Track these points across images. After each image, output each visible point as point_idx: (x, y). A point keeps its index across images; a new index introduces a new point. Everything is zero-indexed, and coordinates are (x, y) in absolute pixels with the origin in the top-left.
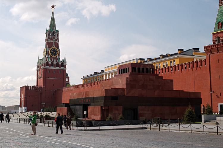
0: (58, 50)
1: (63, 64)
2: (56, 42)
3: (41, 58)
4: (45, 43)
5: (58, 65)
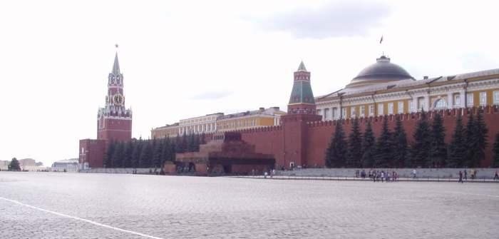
1: (128, 114)
5: (123, 115)
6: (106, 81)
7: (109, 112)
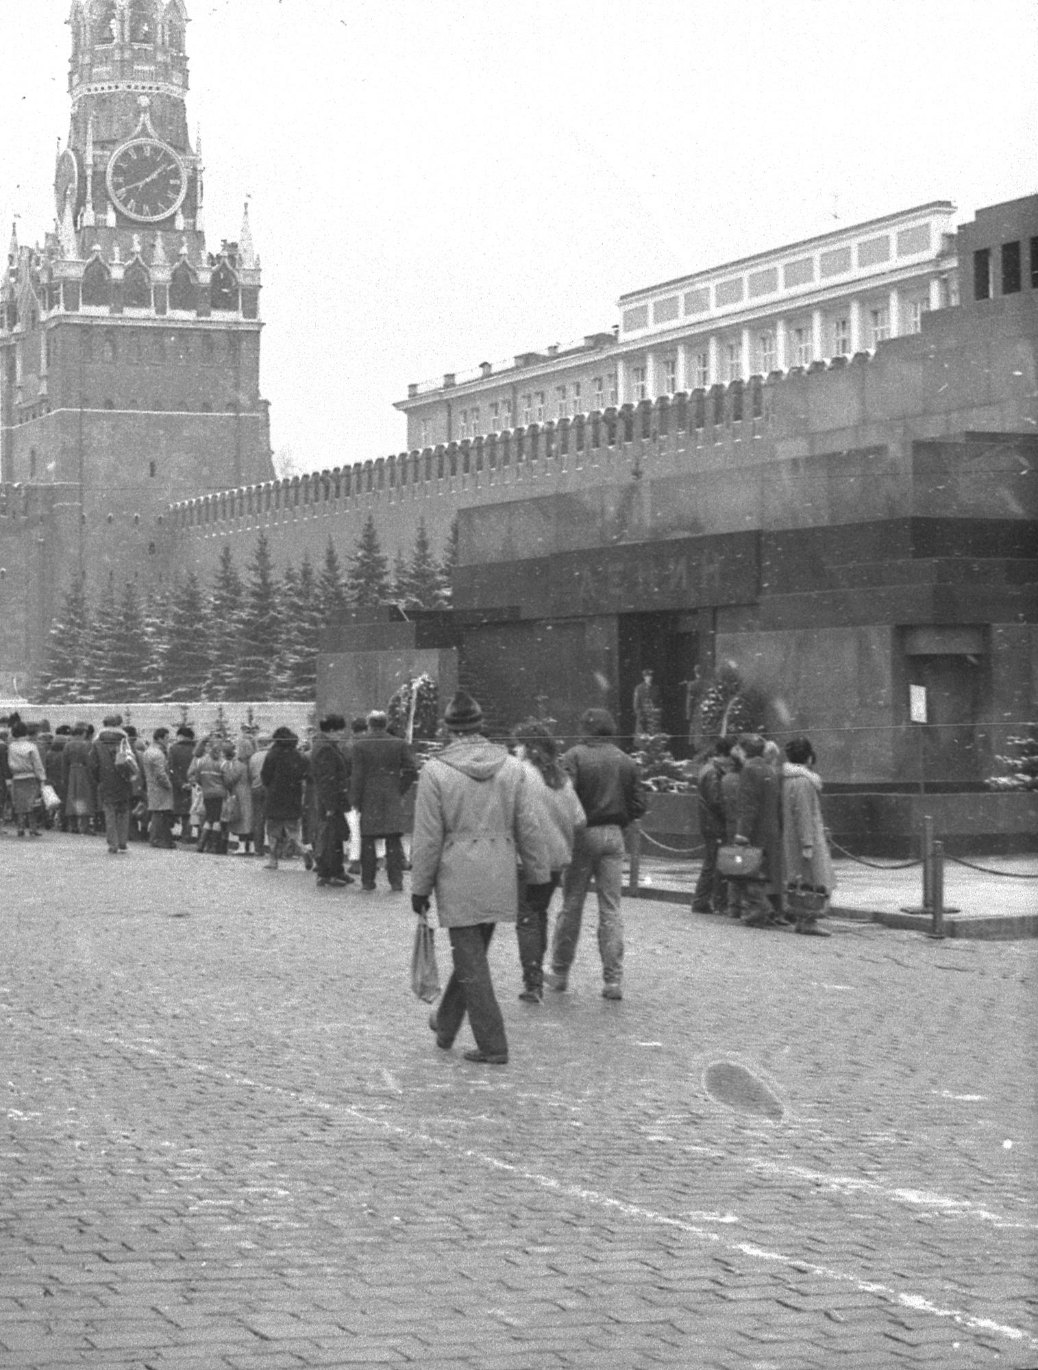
1: (231, 285)
2: (165, 87)
3: (33, 236)
4: (62, 108)
5: (183, 290)
7: (76, 273)
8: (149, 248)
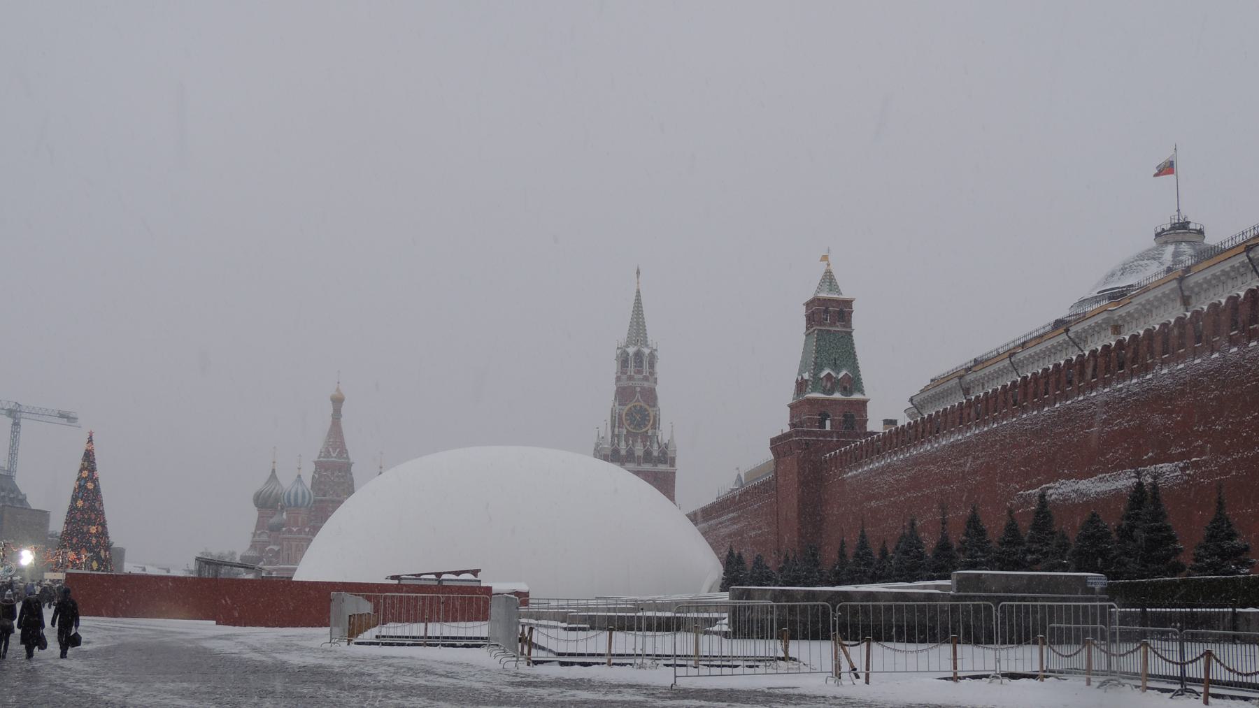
0: (650, 410)
2: (646, 384)
6: (613, 368)
8: (634, 441)
